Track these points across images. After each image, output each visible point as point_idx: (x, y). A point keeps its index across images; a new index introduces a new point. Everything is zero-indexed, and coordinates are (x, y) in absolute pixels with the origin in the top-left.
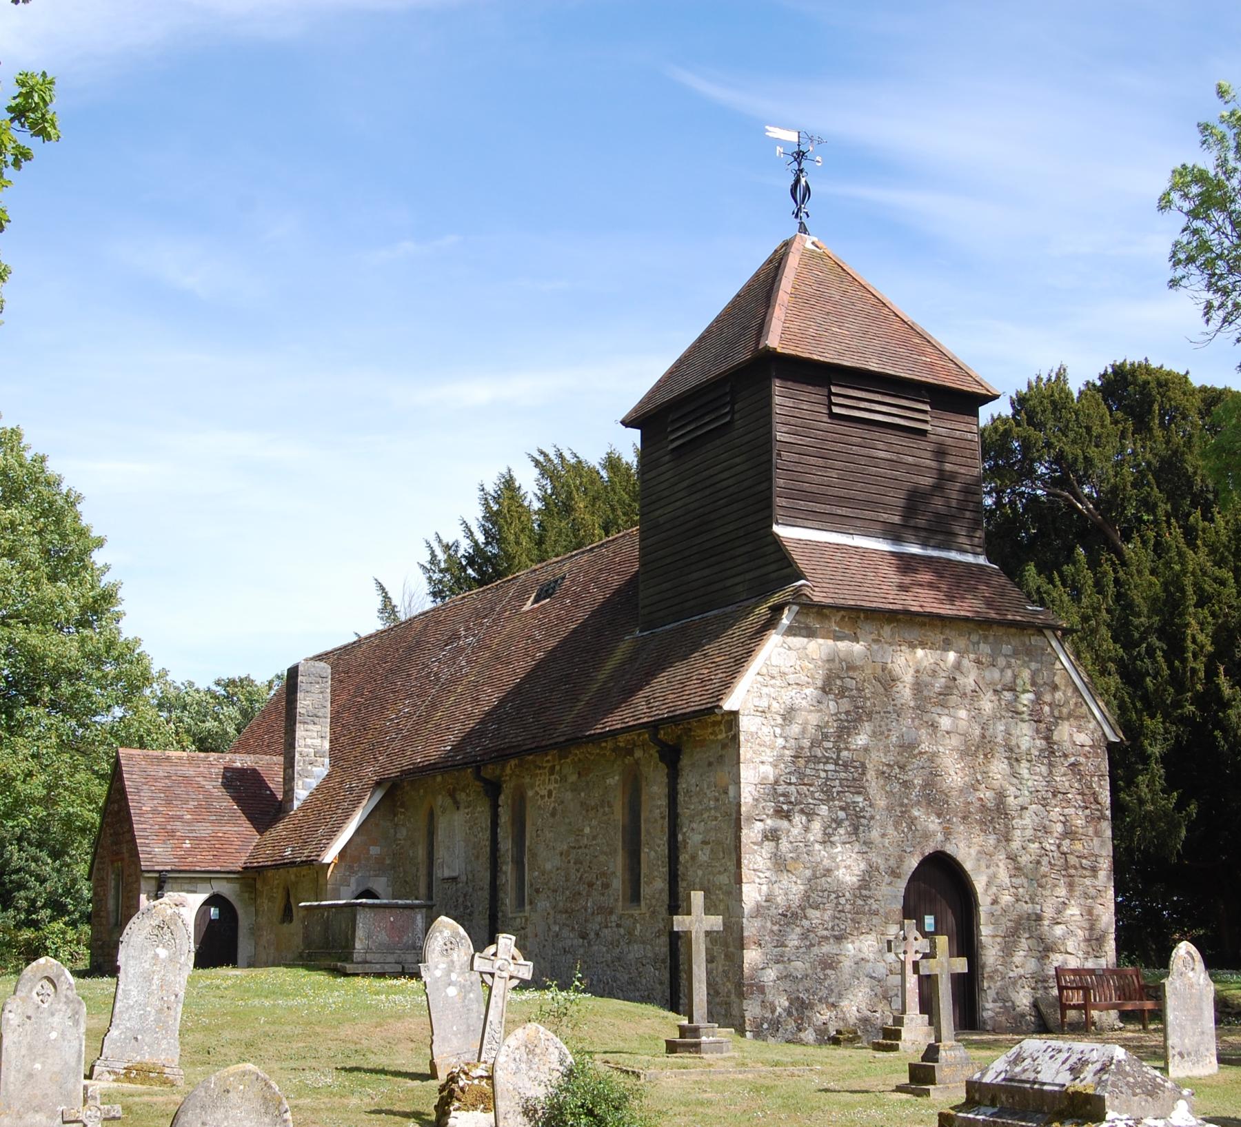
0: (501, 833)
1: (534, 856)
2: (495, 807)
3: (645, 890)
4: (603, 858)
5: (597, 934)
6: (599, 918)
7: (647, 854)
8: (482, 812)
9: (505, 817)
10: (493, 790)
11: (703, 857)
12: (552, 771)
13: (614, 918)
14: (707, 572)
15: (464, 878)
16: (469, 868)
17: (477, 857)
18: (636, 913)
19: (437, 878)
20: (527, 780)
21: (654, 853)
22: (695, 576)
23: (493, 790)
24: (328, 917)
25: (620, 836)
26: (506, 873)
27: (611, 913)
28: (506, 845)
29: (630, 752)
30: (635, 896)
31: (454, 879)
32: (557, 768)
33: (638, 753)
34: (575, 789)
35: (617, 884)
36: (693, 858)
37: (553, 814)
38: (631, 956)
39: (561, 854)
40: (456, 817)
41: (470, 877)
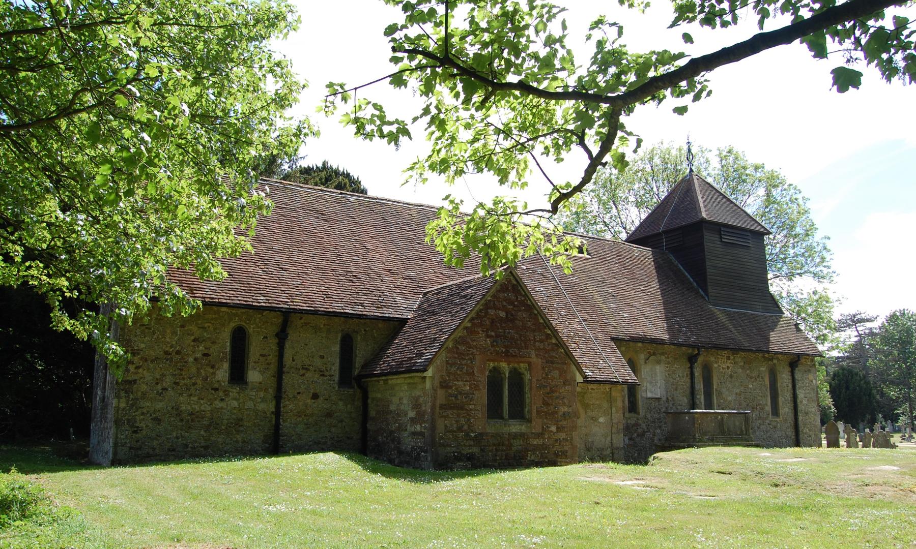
0: (696, 381)
1: (720, 393)
2: (691, 368)
3: (781, 411)
4: (759, 398)
5: (759, 428)
6: (759, 421)
7: (781, 399)
8: (681, 370)
9: (698, 372)
10: (692, 360)
11: (805, 402)
12: (728, 358)
13: (767, 421)
14: (742, 295)
15: (664, 399)
16: (669, 394)
17: (676, 389)
18: (778, 420)
19: (642, 397)
20: (712, 359)
21: (785, 397)
22: (738, 294)
23: (692, 360)
24: (722, 419)
25: (769, 390)
26: (699, 399)
27: (766, 419)
28: (700, 386)
29: (772, 360)
30: (775, 411)
31: (658, 399)
32: (732, 358)
33: (775, 361)
34: (743, 368)
35: (768, 408)
36: (801, 402)
37: (731, 376)
38: (776, 436)
39: (736, 394)
40: (658, 367)
41: (670, 398)
